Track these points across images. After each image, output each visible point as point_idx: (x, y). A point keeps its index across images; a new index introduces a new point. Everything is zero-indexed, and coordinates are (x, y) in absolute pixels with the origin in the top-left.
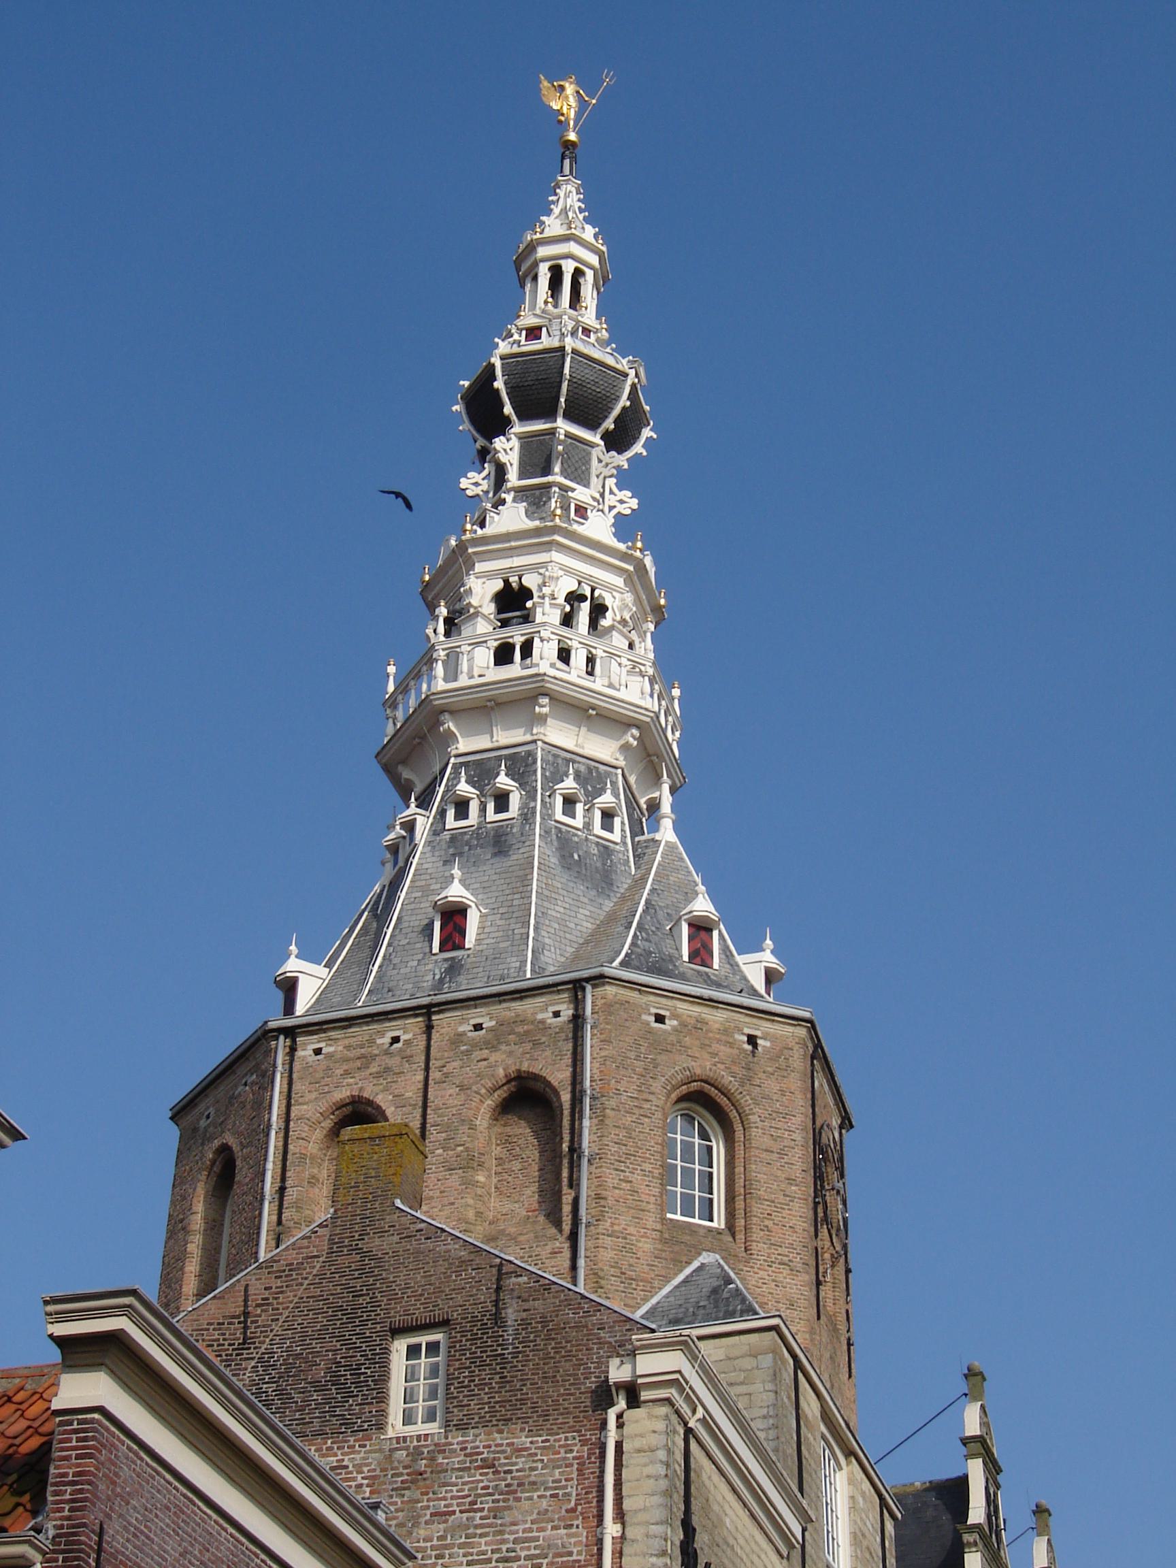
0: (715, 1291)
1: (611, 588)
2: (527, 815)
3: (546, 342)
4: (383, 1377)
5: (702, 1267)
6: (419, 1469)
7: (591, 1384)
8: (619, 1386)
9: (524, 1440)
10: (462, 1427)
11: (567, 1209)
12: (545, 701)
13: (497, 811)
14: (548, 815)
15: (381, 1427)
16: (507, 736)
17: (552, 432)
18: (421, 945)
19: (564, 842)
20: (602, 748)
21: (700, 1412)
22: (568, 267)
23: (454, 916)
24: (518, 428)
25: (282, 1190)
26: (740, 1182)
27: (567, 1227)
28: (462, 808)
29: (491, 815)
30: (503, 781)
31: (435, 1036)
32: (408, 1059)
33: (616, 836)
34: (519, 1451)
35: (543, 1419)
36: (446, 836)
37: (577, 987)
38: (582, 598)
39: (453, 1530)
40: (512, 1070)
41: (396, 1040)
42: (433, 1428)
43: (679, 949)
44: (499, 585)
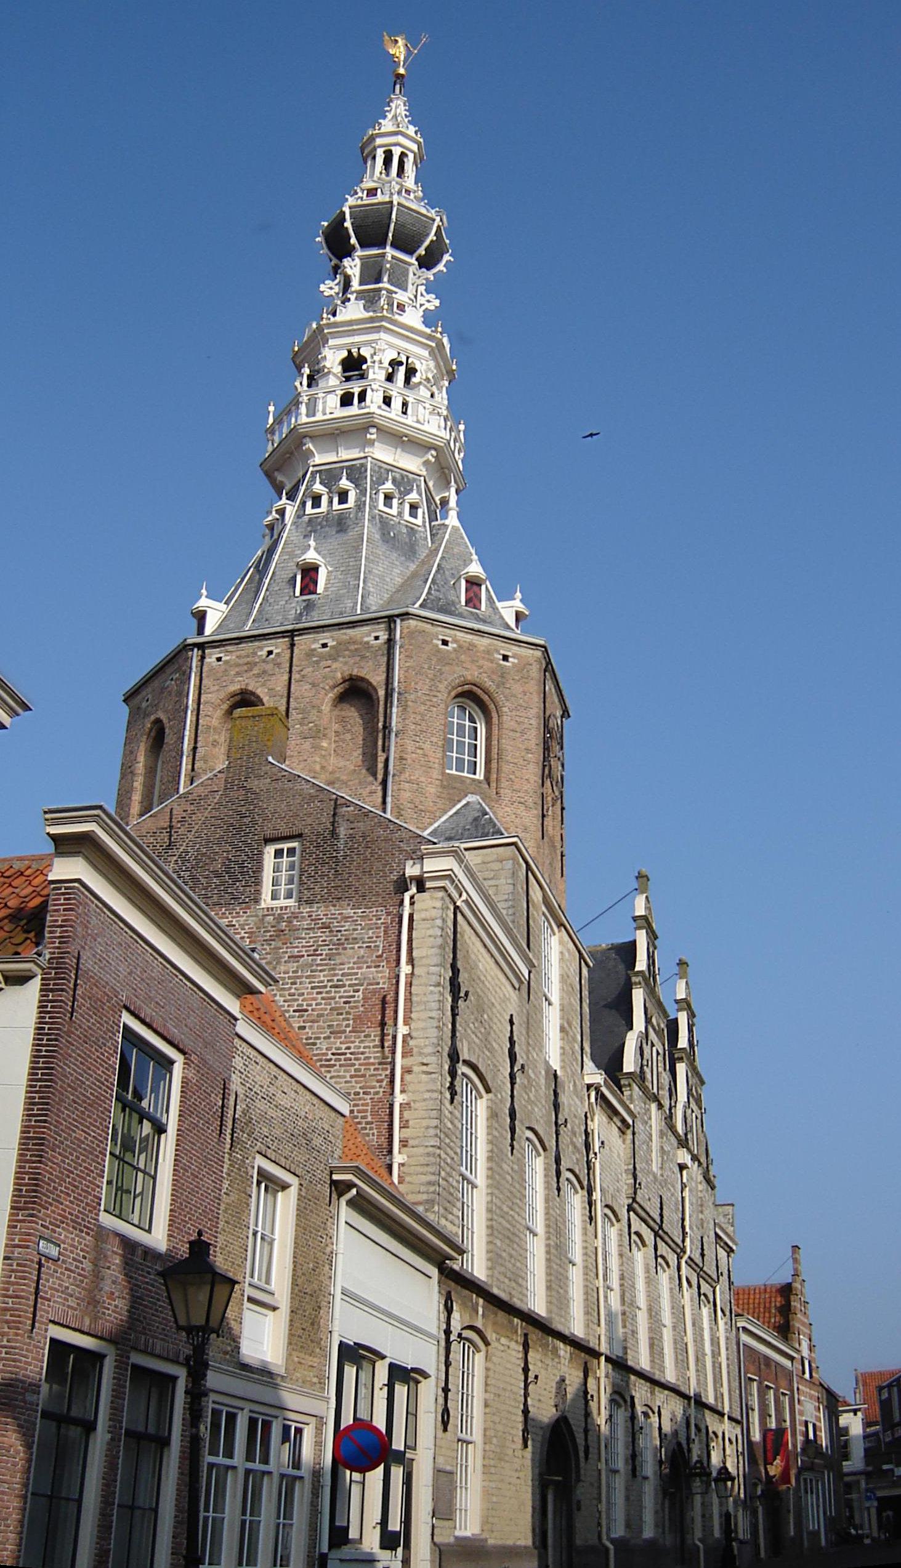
0: (476, 819)
1: (419, 358)
2: (360, 506)
3: (380, 198)
4: (259, 869)
5: (468, 803)
6: (281, 929)
7: (394, 877)
8: (412, 878)
9: (349, 912)
10: (309, 902)
11: (380, 766)
12: (373, 430)
13: (340, 503)
14: (373, 507)
15: (257, 901)
16: (347, 454)
17: (383, 255)
18: (288, 590)
19: (384, 524)
20: (411, 463)
21: (464, 896)
22: (397, 152)
23: (310, 572)
24: (359, 253)
25: (195, 749)
26: (495, 751)
27: (380, 777)
28: (316, 501)
29: (336, 505)
30: (344, 483)
31: (296, 650)
32: (279, 665)
33: (419, 521)
34: (346, 918)
35: (361, 898)
36: (306, 518)
37: (391, 620)
38: (400, 363)
39: (302, 968)
40: (346, 674)
41: (270, 653)
42: (291, 902)
43: (459, 597)
44: (345, 354)
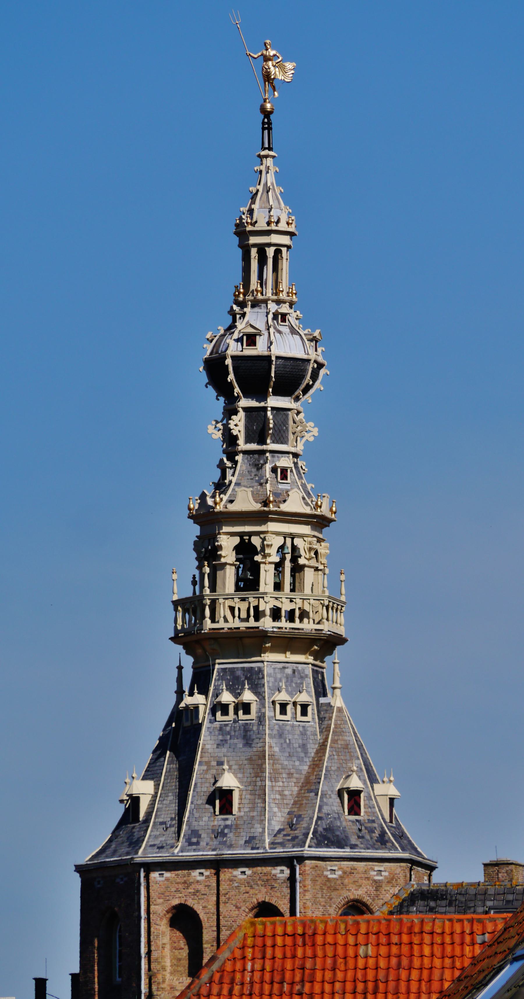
3: (260, 349)
30: (248, 696)
36: (217, 724)
